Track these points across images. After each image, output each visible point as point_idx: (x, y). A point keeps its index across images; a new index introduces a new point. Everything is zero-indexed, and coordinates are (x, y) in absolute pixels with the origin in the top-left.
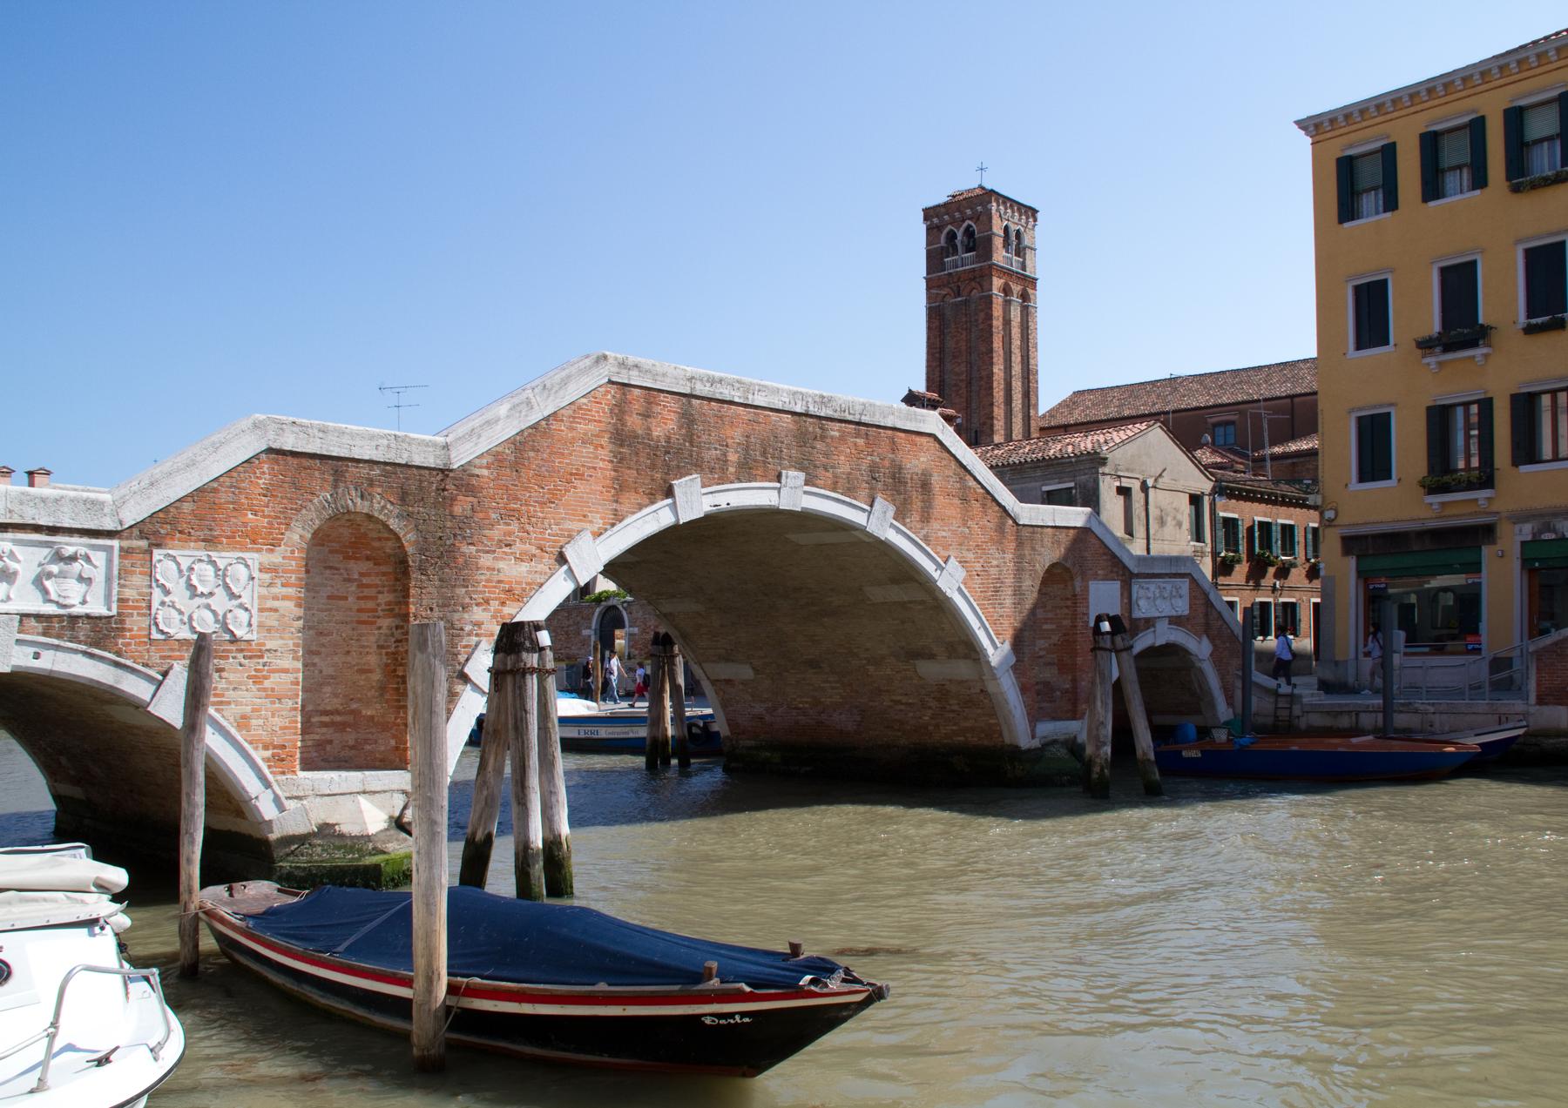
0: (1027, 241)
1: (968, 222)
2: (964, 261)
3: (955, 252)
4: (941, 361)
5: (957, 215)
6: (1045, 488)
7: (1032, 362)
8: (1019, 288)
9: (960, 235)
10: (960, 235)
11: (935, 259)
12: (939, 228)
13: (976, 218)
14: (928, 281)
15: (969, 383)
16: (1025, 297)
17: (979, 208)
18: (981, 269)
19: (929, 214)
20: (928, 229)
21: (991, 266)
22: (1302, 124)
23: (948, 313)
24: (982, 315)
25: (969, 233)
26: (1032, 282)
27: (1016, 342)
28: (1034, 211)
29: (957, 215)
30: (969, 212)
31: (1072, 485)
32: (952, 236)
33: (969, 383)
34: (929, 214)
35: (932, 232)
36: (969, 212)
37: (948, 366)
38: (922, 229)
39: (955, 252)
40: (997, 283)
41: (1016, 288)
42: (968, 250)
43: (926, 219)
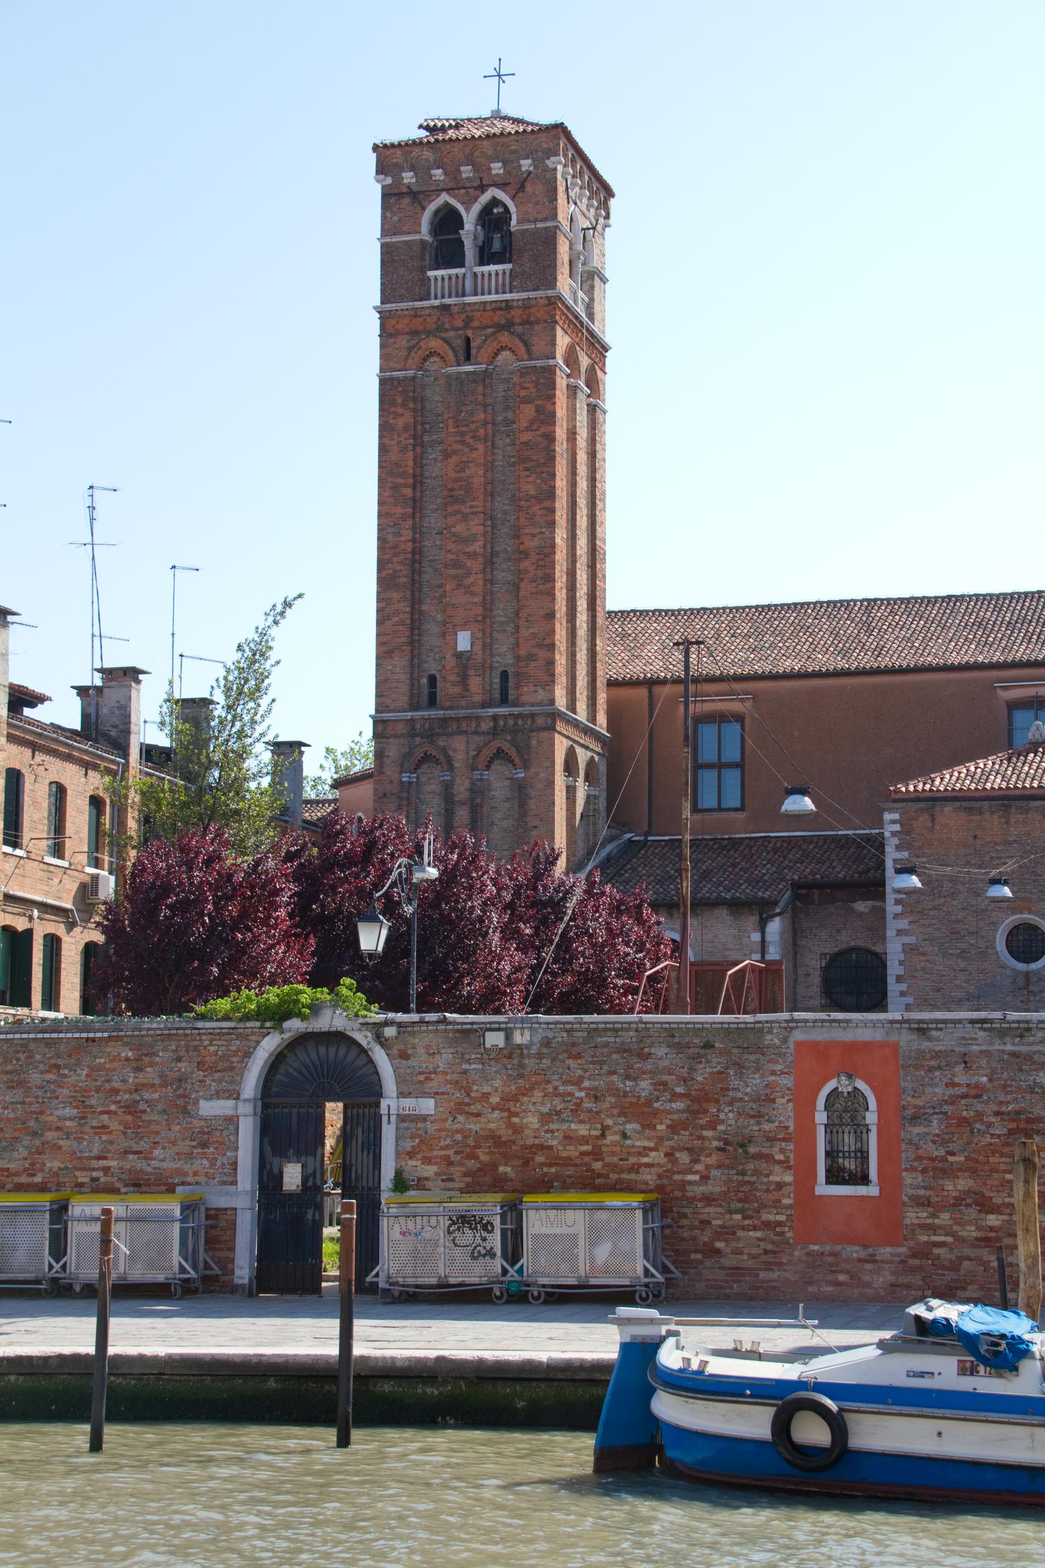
0: (596, 263)
1: (492, 192)
2: (486, 284)
4: (416, 506)
5: (467, 171)
7: (599, 530)
9: (470, 219)
10: (470, 219)
11: (401, 272)
12: (417, 197)
13: (518, 185)
14: (385, 317)
15: (490, 562)
16: (594, 384)
17: (526, 164)
18: (527, 305)
19: (389, 158)
20: (386, 195)
21: (555, 302)
23: (435, 397)
24: (528, 411)
26: (599, 348)
27: (583, 485)
28: (609, 193)
29: (467, 171)
30: (497, 168)
32: (448, 222)
33: (490, 562)
34: (389, 158)
35: (396, 201)
36: (497, 168)
37: (433, 520)
38: (373, 192)
40: (563, 341)
41: (584, 361)
42: (486, 256)
43: (382, 169)
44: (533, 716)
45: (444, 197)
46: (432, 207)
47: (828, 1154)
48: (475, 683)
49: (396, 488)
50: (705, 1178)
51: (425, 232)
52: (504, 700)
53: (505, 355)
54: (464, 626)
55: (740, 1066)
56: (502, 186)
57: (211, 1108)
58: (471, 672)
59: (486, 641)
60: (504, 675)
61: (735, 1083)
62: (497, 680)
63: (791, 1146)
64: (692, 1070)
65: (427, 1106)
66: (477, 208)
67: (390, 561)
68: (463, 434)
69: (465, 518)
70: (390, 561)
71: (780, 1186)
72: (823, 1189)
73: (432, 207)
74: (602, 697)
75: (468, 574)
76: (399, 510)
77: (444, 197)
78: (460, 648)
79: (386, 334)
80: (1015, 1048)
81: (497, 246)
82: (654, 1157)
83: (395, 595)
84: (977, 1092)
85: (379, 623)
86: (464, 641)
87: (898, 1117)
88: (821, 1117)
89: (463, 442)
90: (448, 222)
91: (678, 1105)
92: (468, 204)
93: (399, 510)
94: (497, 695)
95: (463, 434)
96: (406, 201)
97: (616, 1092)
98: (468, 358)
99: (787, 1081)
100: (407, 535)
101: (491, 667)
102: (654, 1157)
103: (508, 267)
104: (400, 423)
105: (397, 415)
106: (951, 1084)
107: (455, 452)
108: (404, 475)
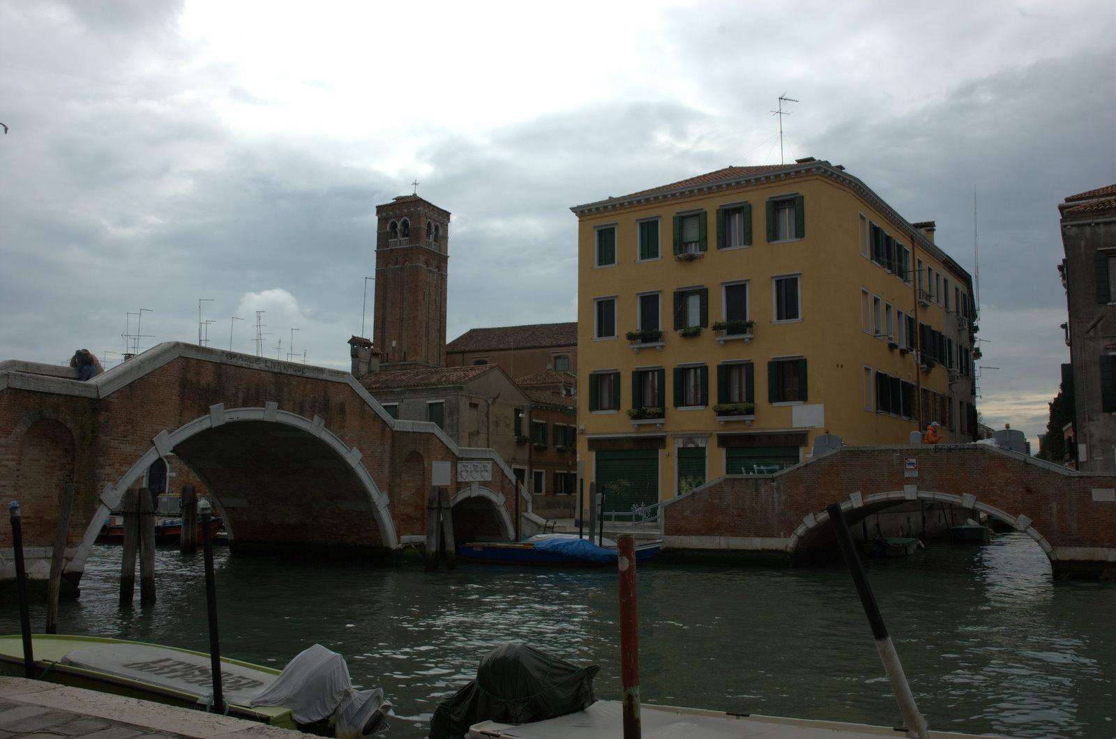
2: (401, 242)
3: (396, 237)
6: (428, 402)
8: (436, 262)
13: (411, 215)
20: (379, 220)
22: (573, 209)
25: (405, 224)
31: (443, 401)
32: (394, 226)
35: (382, 221)
39: (396, 237)
42: (404, 235)
43: (378, 213)
44: (411, 364)
45: (393, 220)
46: (390, 222)
48: (397, 355)
51: (388, 229)
52: (405, 360)
53: (407, 263)
56: (407, 216)
57: (174, 474)
59: (400, 344)
60: (405, 353)
62: (403, 354)
65: (174, 474)
66: (400, 222)
73: (390, 222)
77: (393, 220)
79: (378, 258)
81: (406, 232)
92: (399, 220)
94: (403, 359)
98: (397, 264)
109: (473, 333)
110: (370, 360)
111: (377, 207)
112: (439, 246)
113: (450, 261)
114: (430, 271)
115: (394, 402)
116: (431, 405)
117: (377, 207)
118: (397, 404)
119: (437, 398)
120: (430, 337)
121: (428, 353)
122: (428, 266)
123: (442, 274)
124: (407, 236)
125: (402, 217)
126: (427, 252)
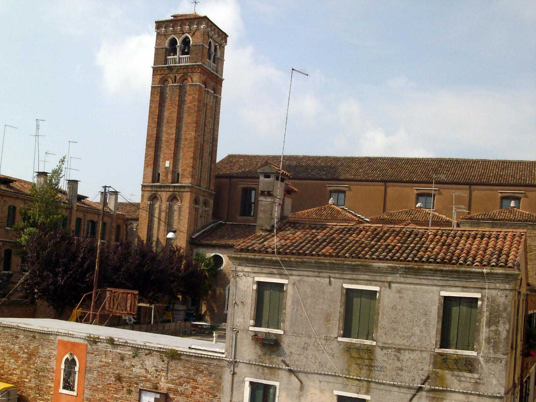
3: (175, 53)
12: (165, 35)
19: (159, 24)
25: (186, 42)
31: (478, 295)
32: (173, 42)
39: (175, 53)
42: (183, 53)
47: (64, 379)
49: (153, 119)
50: (30, 381)
54: (168, 160)
55: (42, 345)
58: (169, 173)
61: (40, 351)
62: (176, 176)
63: (54, 375)
64: (30, 345)
67: (150, 139)
68: (172, 104)
69: (171, 128)
70: (150, 139)
71: (50, 387)
72: (62, 391)
74: (213, 181)
75: (170, 144)
76: (153, 125)
78: (166, 166)
80: (121, 352)
82: (18, 372)
83: (150, 150)
84: (108, 365)
85: (145, 157)
86: (167, 164)
87: (86, 370)
88: (63, 366)
89: (171, 106)
90: (173, 42)
91: (25, 356)
93: (153, 125)
94: (176, 180)
95: (172, 104)
96: (163, 37)
97: (8, 348)
99: (55, 353)
100: (155, 132)
101: (175, 172)
102: (18, 372)
103: (188, 56)
104: (156, 100)
105: (155, 98)
106: (101, 361)
107: (170, 109)
108: (155, 115)
109: (230, 157)
110: (284, 199)
111: (156, 22)
112: (217, 68)
113: (224, 83)
114: (208, 91)
115: (371, 285)
116: (445, 298)
117: (156, 22)
118: (377, 289)
119: (464, 288)
120: (203, 160)
121: (201, 176)
122: (206, 87)
123: (217, 97)
124: (187, 53)
125: (183, 34)
126: (206, 72)
